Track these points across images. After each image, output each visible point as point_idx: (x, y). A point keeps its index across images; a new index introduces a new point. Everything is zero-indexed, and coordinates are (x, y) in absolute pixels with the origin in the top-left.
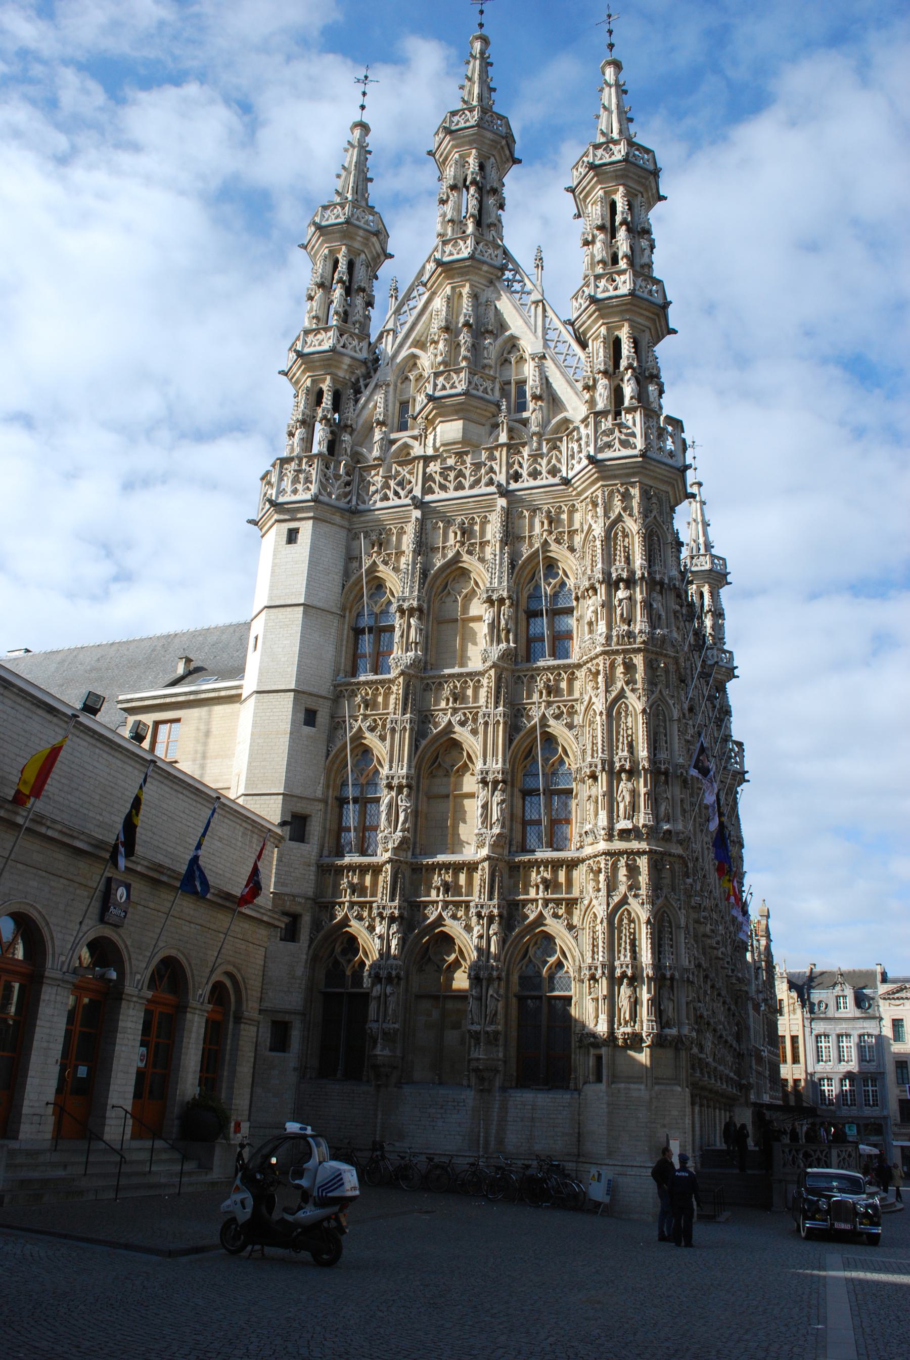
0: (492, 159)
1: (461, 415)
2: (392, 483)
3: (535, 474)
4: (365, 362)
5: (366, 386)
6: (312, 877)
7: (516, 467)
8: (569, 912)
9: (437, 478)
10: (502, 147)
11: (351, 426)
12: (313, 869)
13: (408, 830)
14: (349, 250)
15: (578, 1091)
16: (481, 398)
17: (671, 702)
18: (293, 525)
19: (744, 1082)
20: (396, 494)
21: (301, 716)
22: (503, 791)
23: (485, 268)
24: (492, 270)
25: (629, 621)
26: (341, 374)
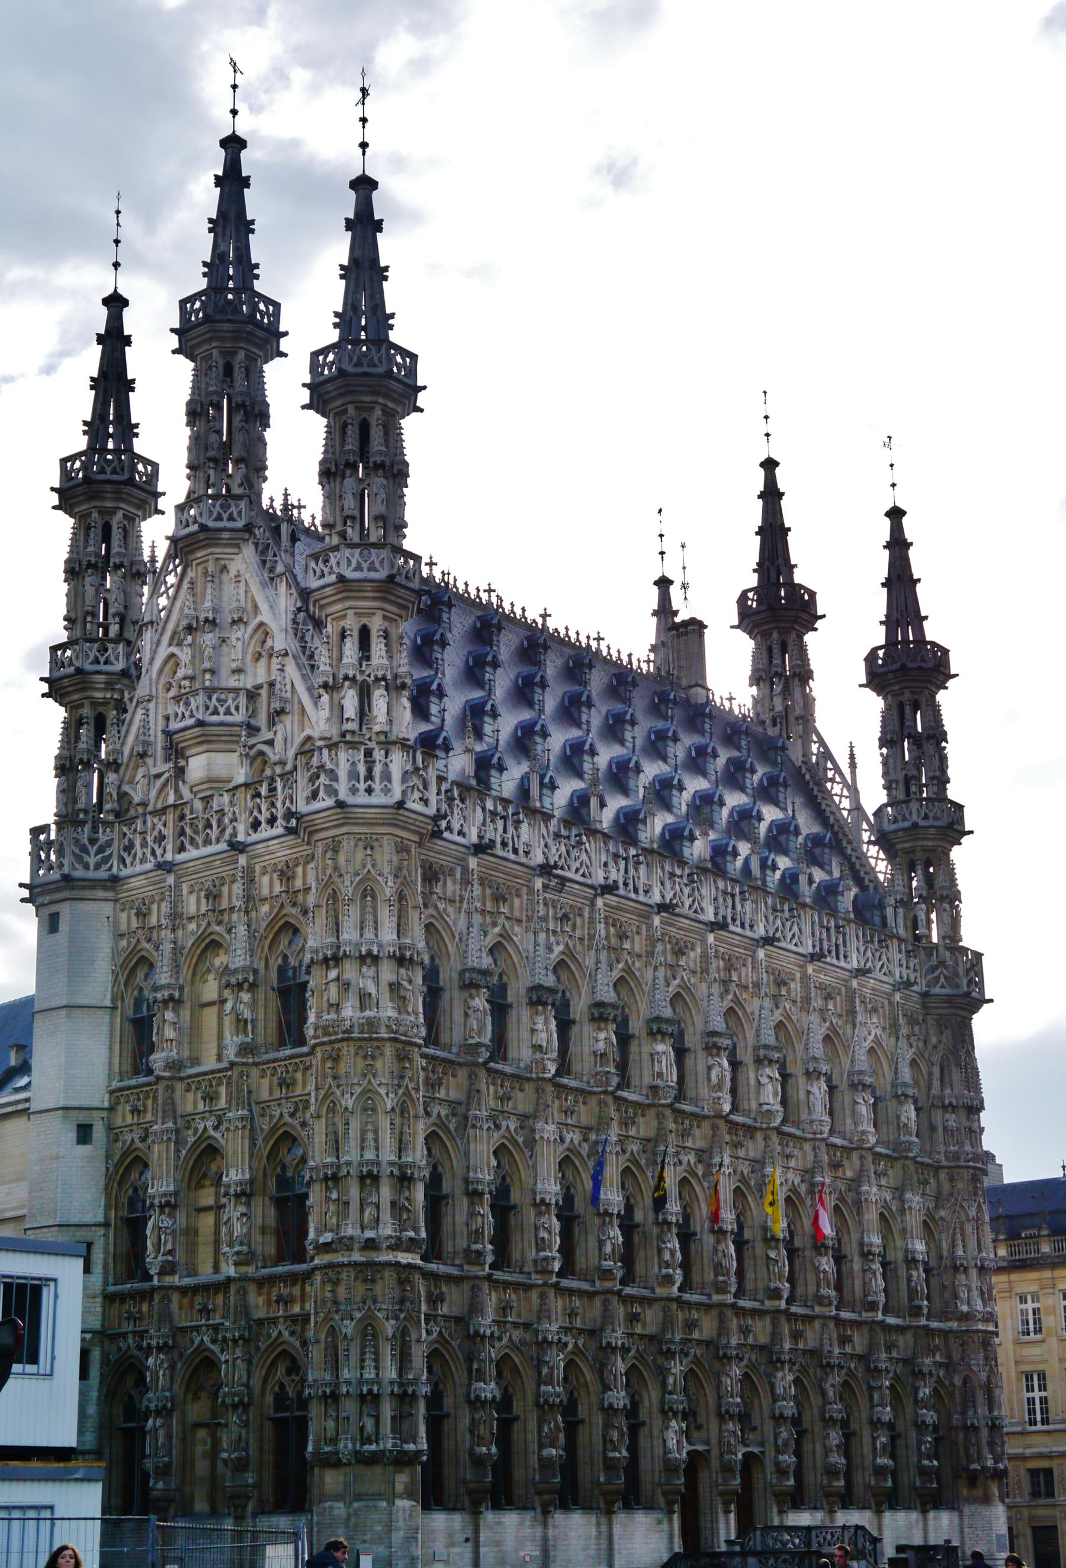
0: (241, 354)
1: (205, 747)
2: (149, 839)
3: (272, 821)
4: (125, 673)
5: (131, 700)
6: (99, 1309)
7: (255, 813)
8: (303, 1330)
9: (188, 830)
10: (250, 333)
11: (115, 761)
12: (99, 1300)
13: (170, 1252)
14: (102, 512)
15: (311, 1511)
16: (222, 724)
17: (382, 1091)
18: (54, 908)
19: (975, 1466)
20: (153, 853)
21: (73, 1135)
22: (248, 1204)
23: (226, 535)
24: (234, 535)
25: (337, 1007)
26: (98, 695)
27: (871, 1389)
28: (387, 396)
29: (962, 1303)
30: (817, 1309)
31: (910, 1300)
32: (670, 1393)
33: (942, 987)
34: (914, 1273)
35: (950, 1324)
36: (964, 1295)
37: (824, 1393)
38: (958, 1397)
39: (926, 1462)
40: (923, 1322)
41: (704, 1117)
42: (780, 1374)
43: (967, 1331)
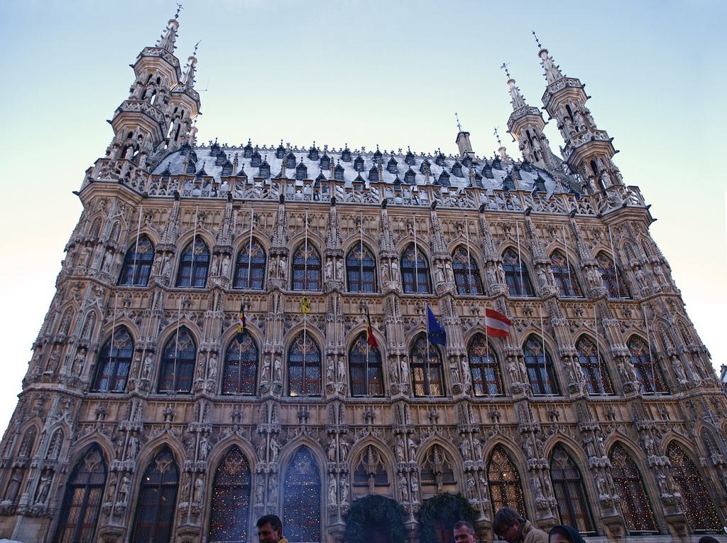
27: (585, 445)
28: (149, 64)
29: (681, 379)
30: (514, 397)
31: (623, 382)
32: (331, 460)
33: (610, 209)
34: (622, 365)
35: (677, 395)
36: (681, 372)
37: (526, 453)
38: (701, 446)
39: (666, 495)
40: (637, 394)
41: (383, 297)
42: (466, 441)
43: (692, 396)
